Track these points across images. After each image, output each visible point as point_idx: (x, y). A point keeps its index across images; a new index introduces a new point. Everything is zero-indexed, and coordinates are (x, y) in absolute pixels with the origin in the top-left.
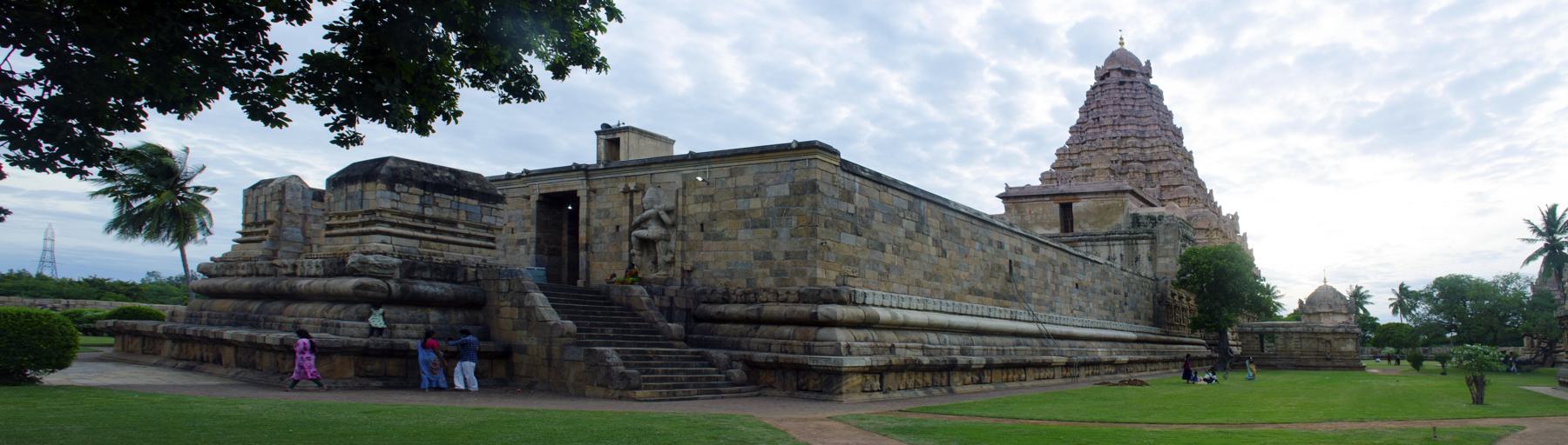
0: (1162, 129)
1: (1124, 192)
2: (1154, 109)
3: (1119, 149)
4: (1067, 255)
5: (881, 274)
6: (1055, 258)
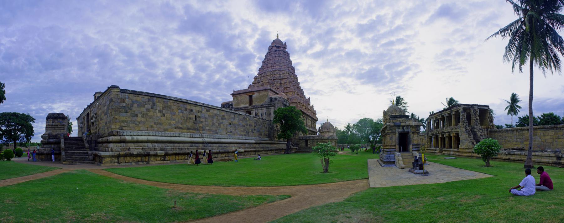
0: (287, 67)
1: (268, 89)
2: (285, 60)
3: (273, 75)
4: (225, 112)
5: (136, 125)
6: (218, 113)
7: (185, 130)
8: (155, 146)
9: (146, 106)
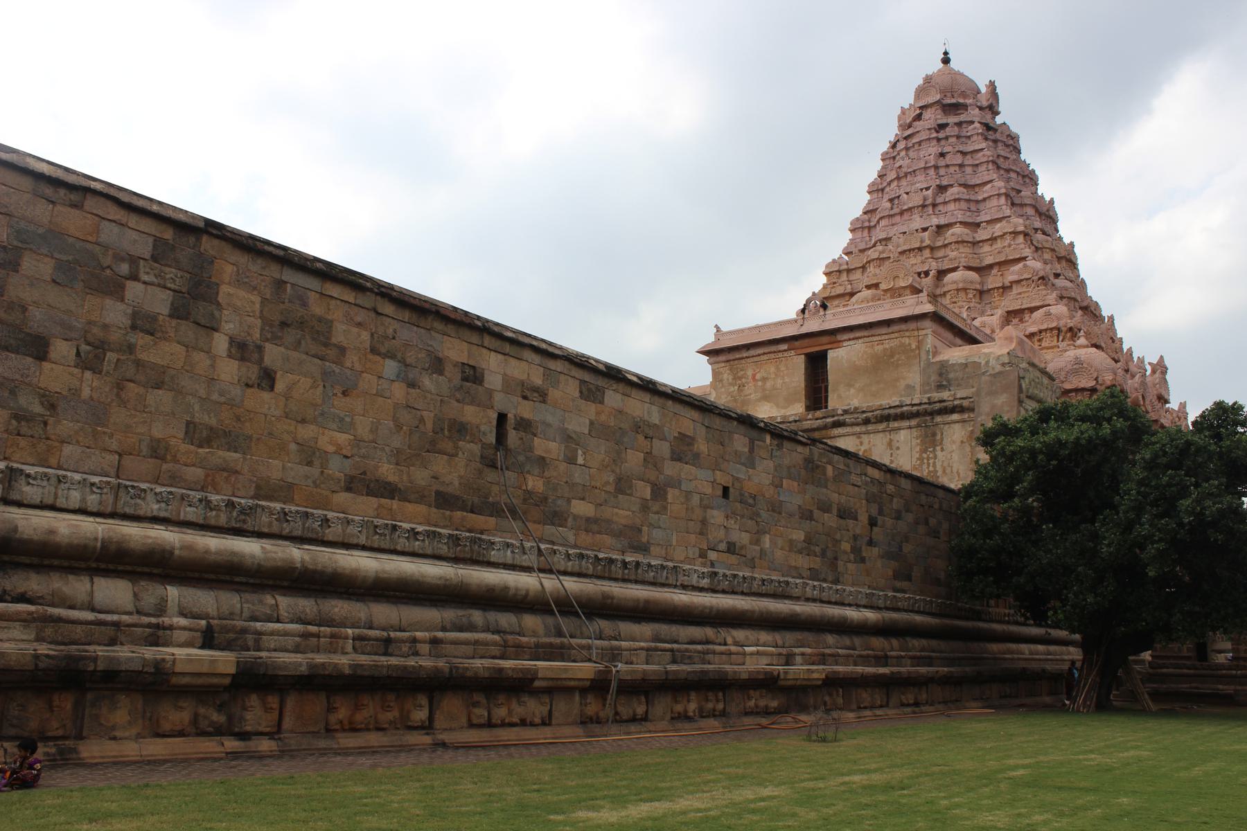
6: (655, 418)
7: (422, 509)
8: (161, 610)
9: (134, 290)
